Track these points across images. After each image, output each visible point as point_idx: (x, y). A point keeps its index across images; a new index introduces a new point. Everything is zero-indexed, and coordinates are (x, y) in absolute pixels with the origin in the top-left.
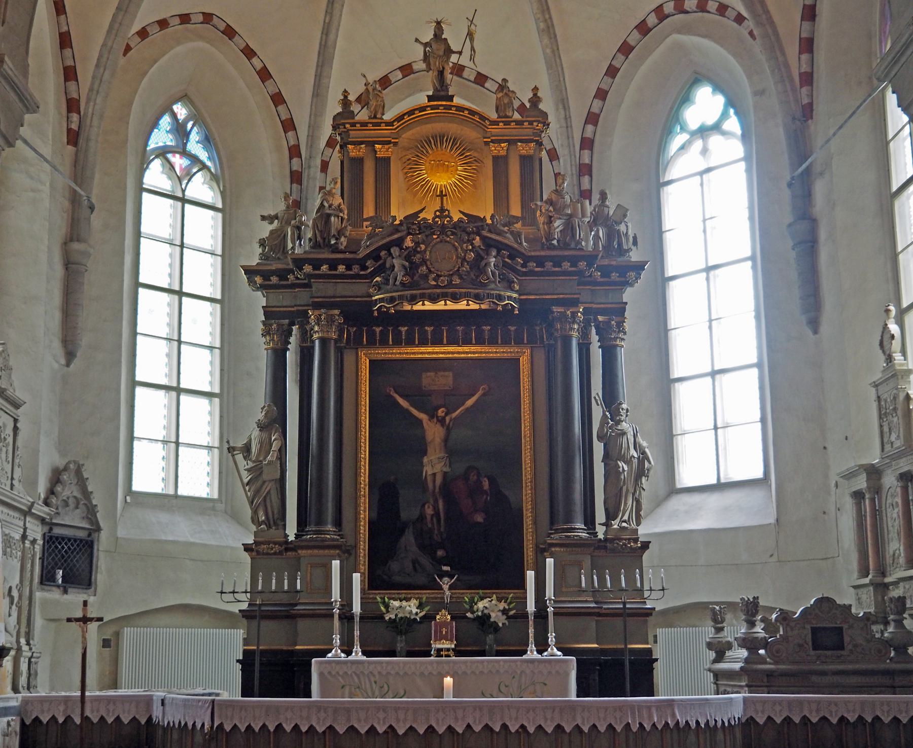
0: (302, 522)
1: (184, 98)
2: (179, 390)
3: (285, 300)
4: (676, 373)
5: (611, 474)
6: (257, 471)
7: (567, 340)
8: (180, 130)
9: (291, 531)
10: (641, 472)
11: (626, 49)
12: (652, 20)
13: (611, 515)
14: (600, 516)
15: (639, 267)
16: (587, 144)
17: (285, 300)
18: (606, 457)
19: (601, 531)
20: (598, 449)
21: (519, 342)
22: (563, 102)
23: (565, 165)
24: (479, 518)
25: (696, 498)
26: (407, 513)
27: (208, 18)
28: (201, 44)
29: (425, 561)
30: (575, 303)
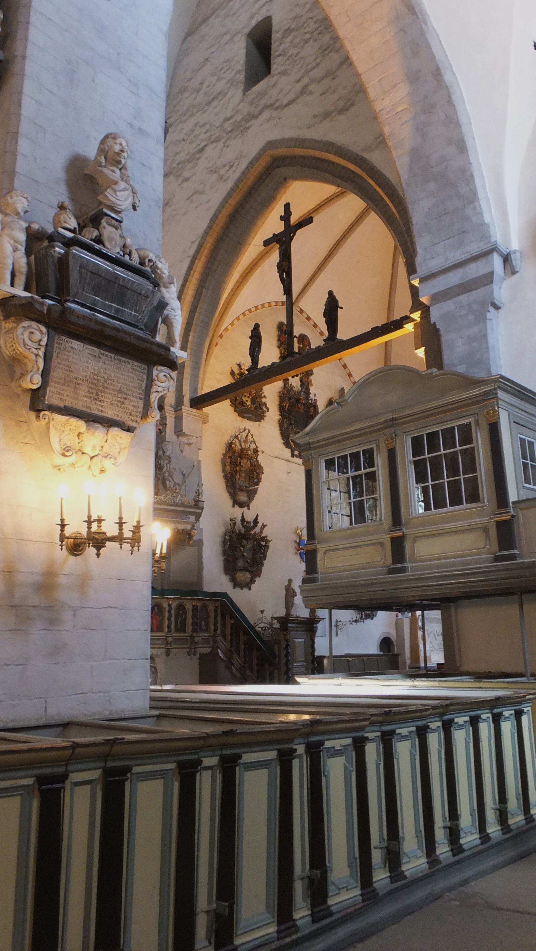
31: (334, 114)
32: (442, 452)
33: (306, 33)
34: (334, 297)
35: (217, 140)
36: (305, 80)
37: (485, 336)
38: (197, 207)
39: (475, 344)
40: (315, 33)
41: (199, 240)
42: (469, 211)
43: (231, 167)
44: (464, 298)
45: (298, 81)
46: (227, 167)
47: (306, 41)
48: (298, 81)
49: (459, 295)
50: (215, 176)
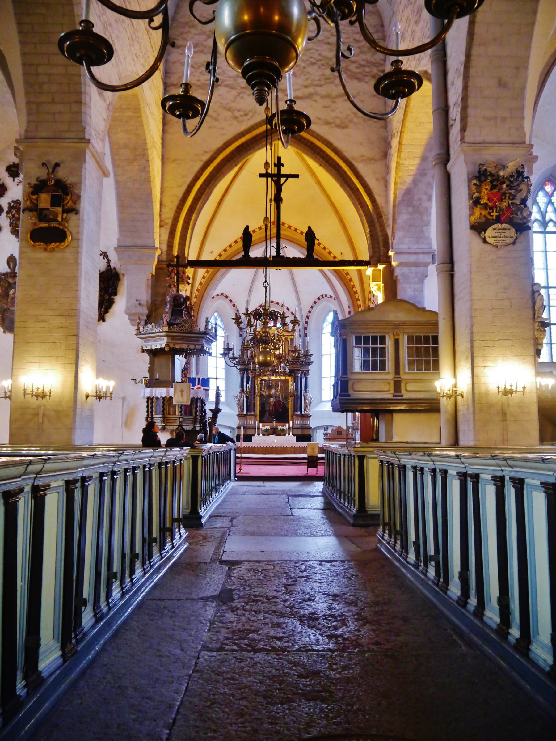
0: (247, 410)
1: (216, 311)
2: (216, 378)
3: (243, 367)
4: (323, 376)
5: (305, 402)
6: (239, 401)
7: (298, 377)
8: (216, 319)
9: (245, 412)
10: (310, 403)
11: (315, 303)
12: (321, 297)
13: (305, 410)
14: (303, 410)
15: (312, 362)
16: (306, 323)
17: (243, 367)
18: (304, 399)
19: (303, 413)
20: (303, 398)
21: (289, 376)
22: (301, 314)
23: (301, 327)
24: (280, 410)
25: (326, 403)
26: (267, 409)
27: (222, 294)
28: (221, 301)
29: (270, 418)
30: (299, 370)
31: (333, 125)
32: (423, 345)
33: (312, 57)
34: (313, 232)
35: (231, 87)
36: (311, 90)
37: (422, 291)
38: (210, 127)
39: (417, 293)
40: (319, 63)
41: (212, 153)
42: (425, 229)
43: (246, 115)
44: (413, 269)
45: (306, 87)
46: (242, 113)
47: (312, 64)
48: (306, 87)
49: (411, 266)
50: (229, 114)
